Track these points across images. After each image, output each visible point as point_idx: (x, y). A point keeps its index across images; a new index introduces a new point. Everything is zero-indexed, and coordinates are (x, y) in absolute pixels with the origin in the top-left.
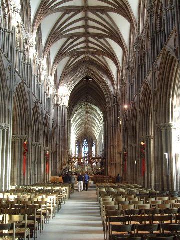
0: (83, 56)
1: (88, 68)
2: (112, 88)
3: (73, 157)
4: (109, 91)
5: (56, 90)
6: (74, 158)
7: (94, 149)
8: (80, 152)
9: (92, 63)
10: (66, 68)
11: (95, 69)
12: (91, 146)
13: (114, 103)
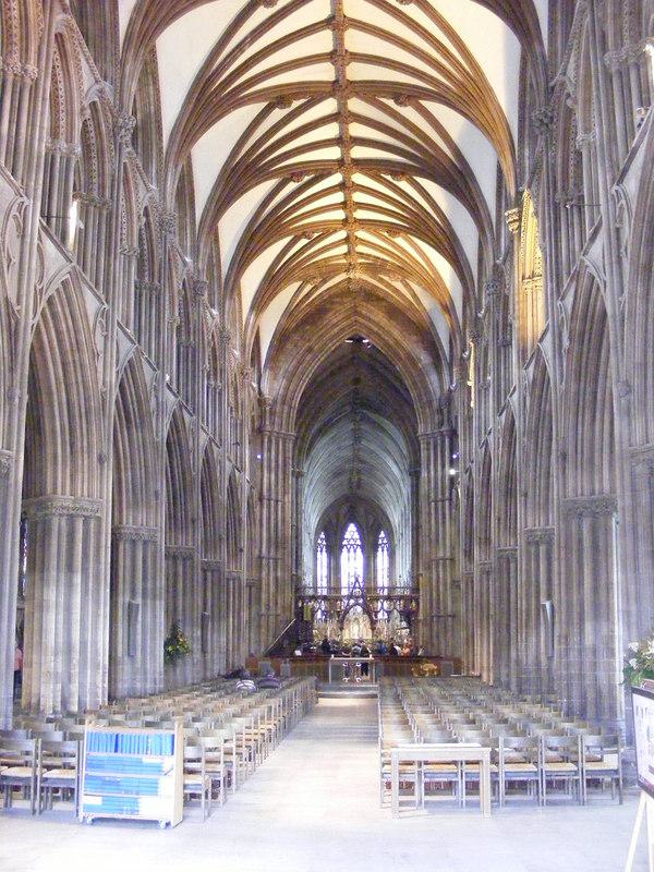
0: (343, 276)
1: (357, 313)
2: (433, 378)
3: (310, 592)
4: (426, 388)
5: (255, 385)
6: (314, 598)
7: (382, 558)
8: (335, 569)
9: (371, 296)
10: (289, 313)
11: (379, 317)
12: (370, 548)
13: (441, 424)
